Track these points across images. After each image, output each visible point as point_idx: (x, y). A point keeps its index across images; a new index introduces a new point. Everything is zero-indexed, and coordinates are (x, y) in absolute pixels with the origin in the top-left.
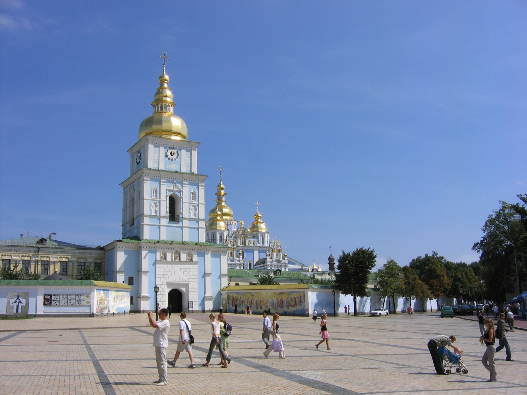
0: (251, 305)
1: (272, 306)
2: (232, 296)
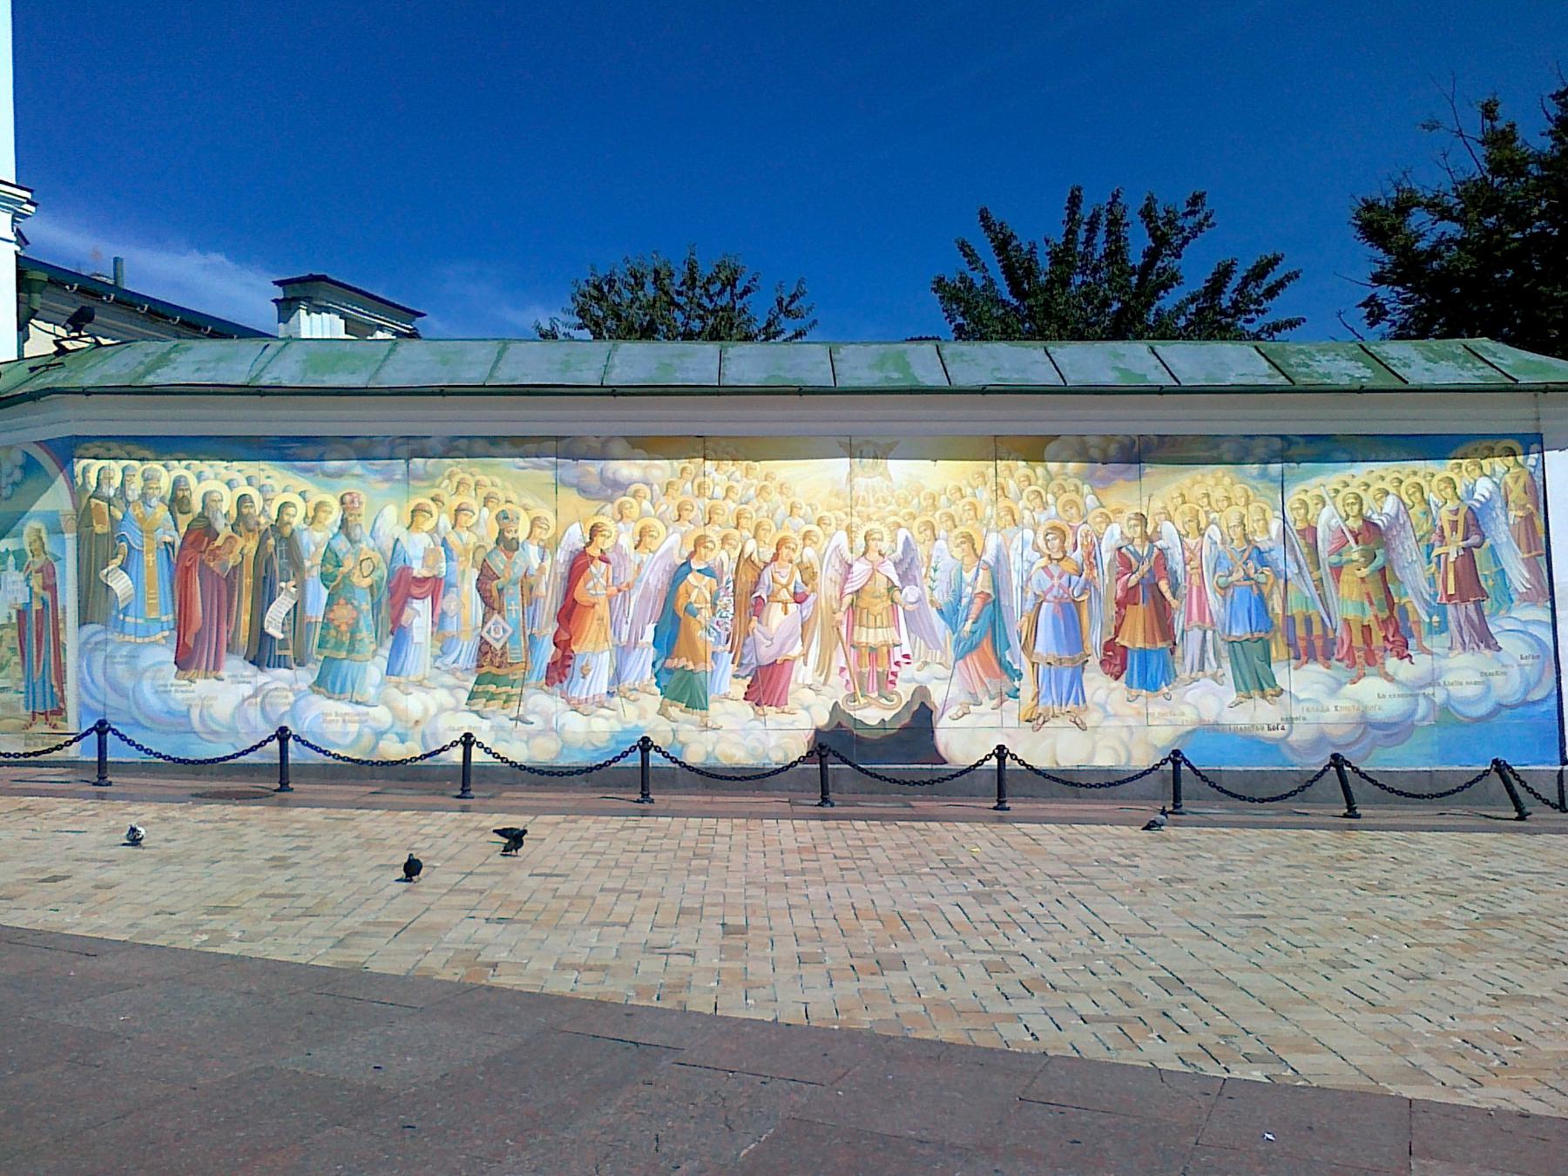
0: (563, 646)
1: (965, 649)
2: (177, 502)
